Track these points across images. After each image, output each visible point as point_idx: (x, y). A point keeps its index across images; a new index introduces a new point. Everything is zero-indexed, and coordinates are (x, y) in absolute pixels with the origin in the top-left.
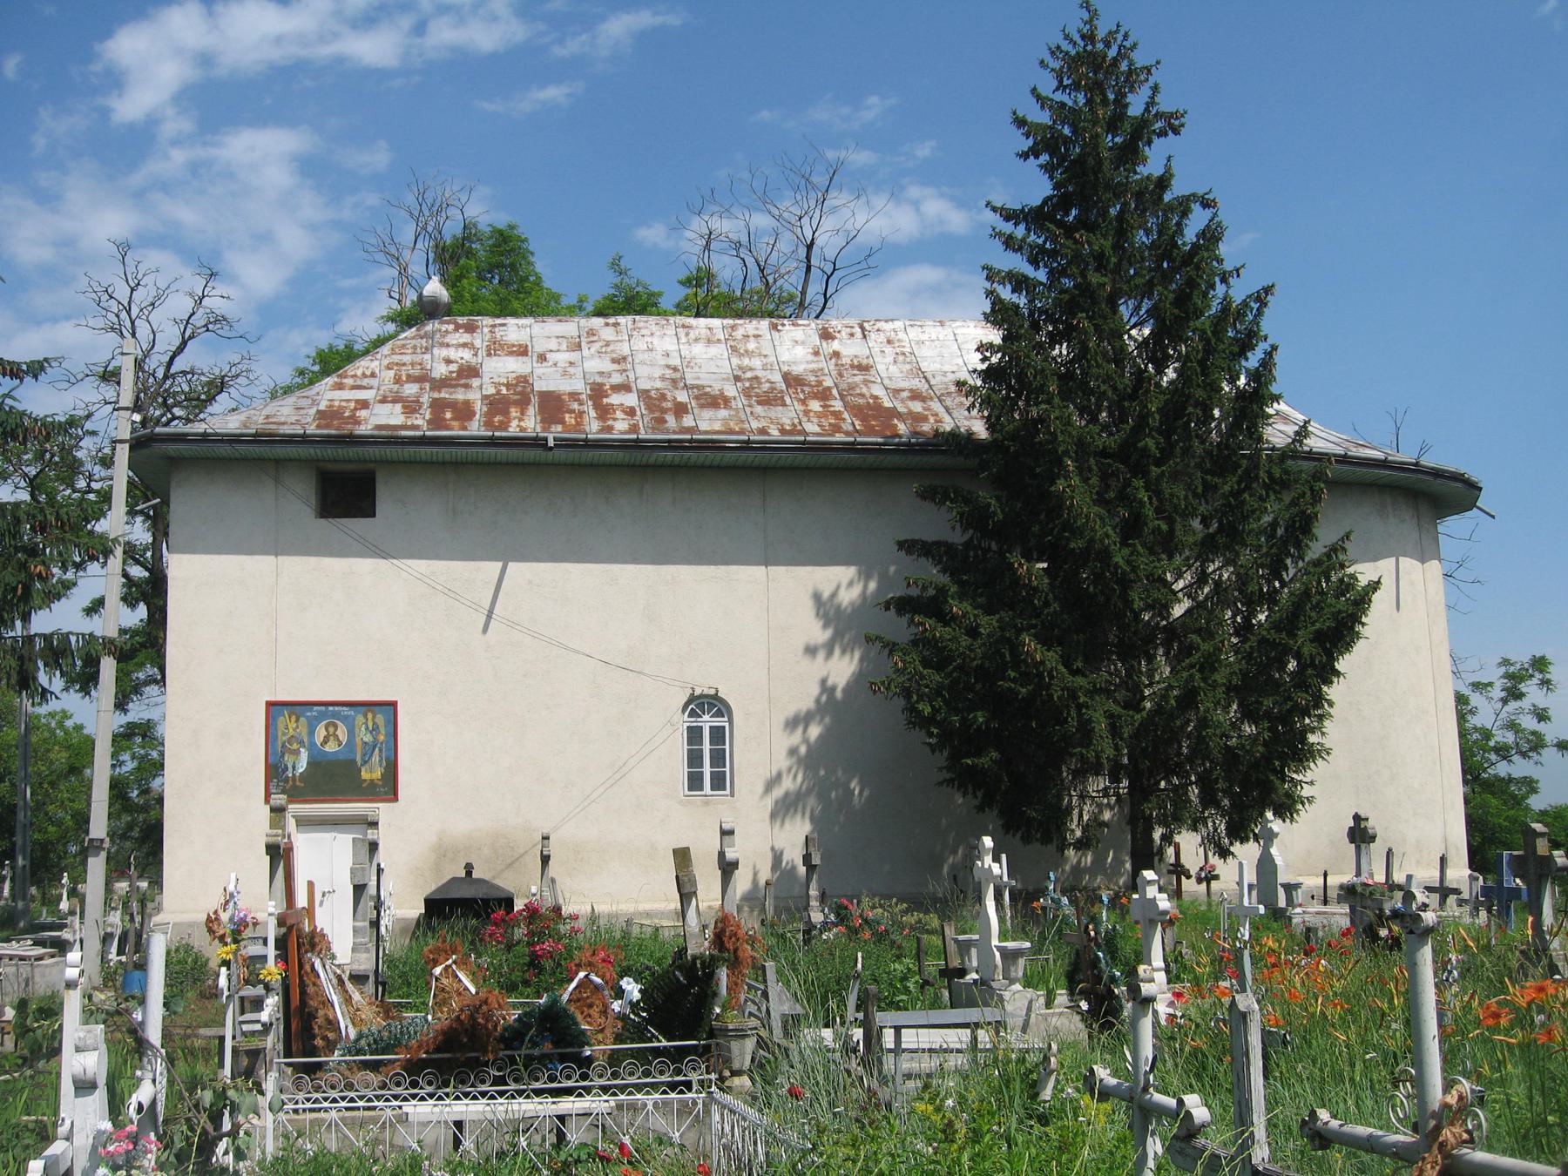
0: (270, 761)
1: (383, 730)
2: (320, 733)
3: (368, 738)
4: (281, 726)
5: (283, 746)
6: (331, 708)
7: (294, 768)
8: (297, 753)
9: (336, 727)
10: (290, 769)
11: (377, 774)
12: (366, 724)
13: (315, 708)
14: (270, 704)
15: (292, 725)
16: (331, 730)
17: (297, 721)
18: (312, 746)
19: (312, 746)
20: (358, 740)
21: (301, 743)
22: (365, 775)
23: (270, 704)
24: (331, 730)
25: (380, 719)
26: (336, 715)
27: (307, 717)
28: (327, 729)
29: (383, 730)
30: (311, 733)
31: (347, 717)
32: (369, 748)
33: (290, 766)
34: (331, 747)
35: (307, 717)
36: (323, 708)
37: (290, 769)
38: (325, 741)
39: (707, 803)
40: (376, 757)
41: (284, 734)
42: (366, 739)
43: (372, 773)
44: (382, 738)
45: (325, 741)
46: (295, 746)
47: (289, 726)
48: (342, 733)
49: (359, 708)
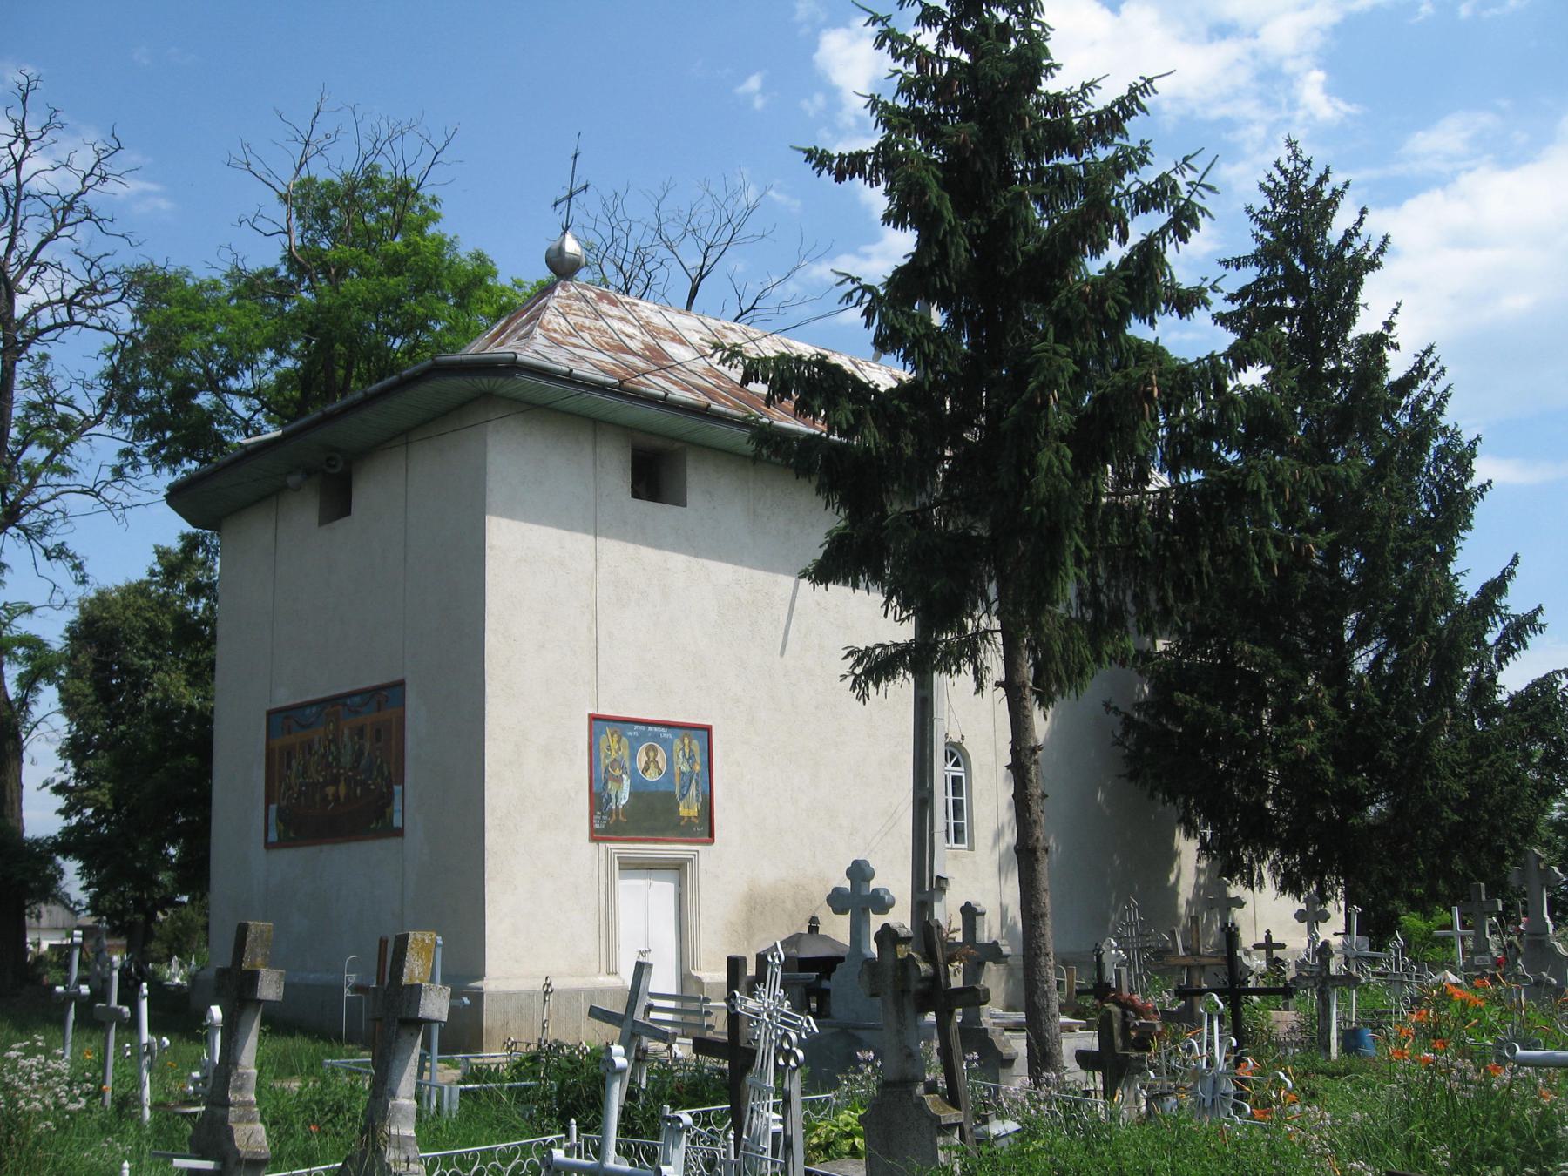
0: (595, 789)
1: (697, 758)
2: (642, 758)
3: (685, 768)
4: (603, 746)
5: (606, 771)
6: (650, 728)
7: (617, 798)
8: (619, 780)
9: (655, 750)
10: (614, 800)
11: (694, 812)
12: (683, 749)
13: (636, 727)
14: (593, 718)
15: (615, 746)
16: (652, 754)
17: (619, 742)
18: (633, 774)
19: (633, 774)
20: (676, 768)
21: (623, 768)
22: (683, 812)
23: (593, 718)
24: (652, 754)
25: (696, 745)
26: (655, 737)
27: (629, 737)
28: (647, 754)
29: (697, 758)
30: (633, 757)
31: (665, 740)
32: (688, 778)
33: (613, 796)
34: (652, 776)
35: (629, 737)
36: (642, 728)
37: (614, 800)
38: (646, 769)
39: (955, 857)
40: (693, 792)
41: (606, 757)
42: (683, 769)
43: (689, 809)
44: (697, 768)
45: (646, 769)
46: (618, 772)
47: (613, 747)
48: (661, 759)
49: (677, 731)
